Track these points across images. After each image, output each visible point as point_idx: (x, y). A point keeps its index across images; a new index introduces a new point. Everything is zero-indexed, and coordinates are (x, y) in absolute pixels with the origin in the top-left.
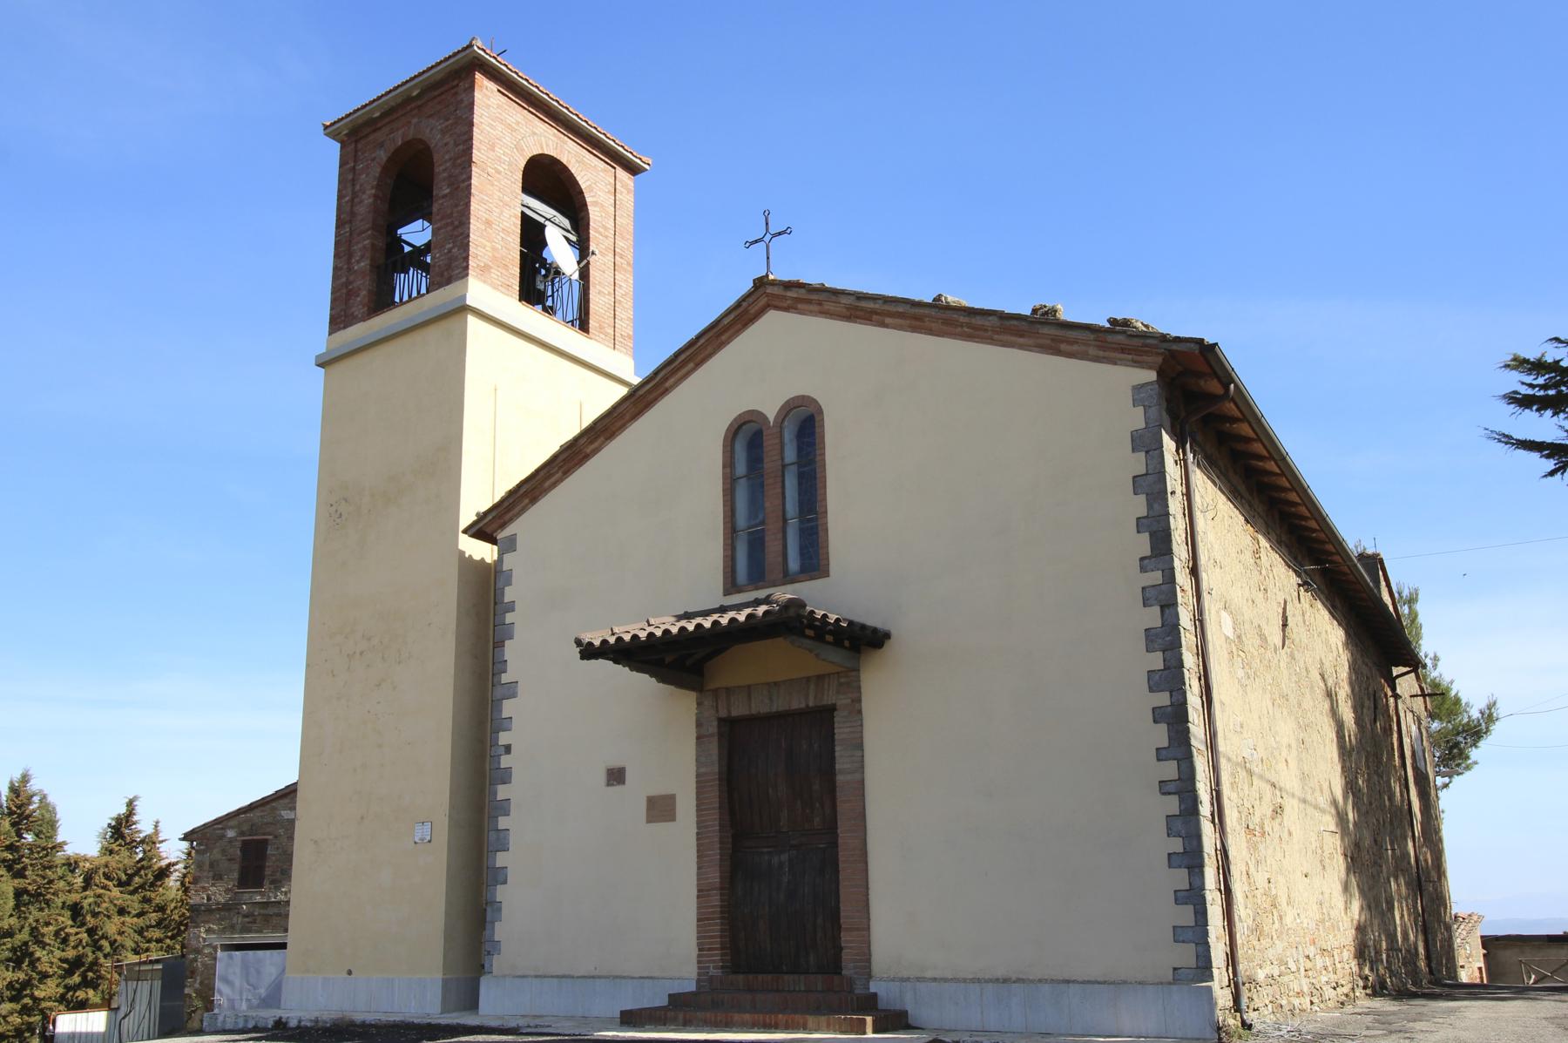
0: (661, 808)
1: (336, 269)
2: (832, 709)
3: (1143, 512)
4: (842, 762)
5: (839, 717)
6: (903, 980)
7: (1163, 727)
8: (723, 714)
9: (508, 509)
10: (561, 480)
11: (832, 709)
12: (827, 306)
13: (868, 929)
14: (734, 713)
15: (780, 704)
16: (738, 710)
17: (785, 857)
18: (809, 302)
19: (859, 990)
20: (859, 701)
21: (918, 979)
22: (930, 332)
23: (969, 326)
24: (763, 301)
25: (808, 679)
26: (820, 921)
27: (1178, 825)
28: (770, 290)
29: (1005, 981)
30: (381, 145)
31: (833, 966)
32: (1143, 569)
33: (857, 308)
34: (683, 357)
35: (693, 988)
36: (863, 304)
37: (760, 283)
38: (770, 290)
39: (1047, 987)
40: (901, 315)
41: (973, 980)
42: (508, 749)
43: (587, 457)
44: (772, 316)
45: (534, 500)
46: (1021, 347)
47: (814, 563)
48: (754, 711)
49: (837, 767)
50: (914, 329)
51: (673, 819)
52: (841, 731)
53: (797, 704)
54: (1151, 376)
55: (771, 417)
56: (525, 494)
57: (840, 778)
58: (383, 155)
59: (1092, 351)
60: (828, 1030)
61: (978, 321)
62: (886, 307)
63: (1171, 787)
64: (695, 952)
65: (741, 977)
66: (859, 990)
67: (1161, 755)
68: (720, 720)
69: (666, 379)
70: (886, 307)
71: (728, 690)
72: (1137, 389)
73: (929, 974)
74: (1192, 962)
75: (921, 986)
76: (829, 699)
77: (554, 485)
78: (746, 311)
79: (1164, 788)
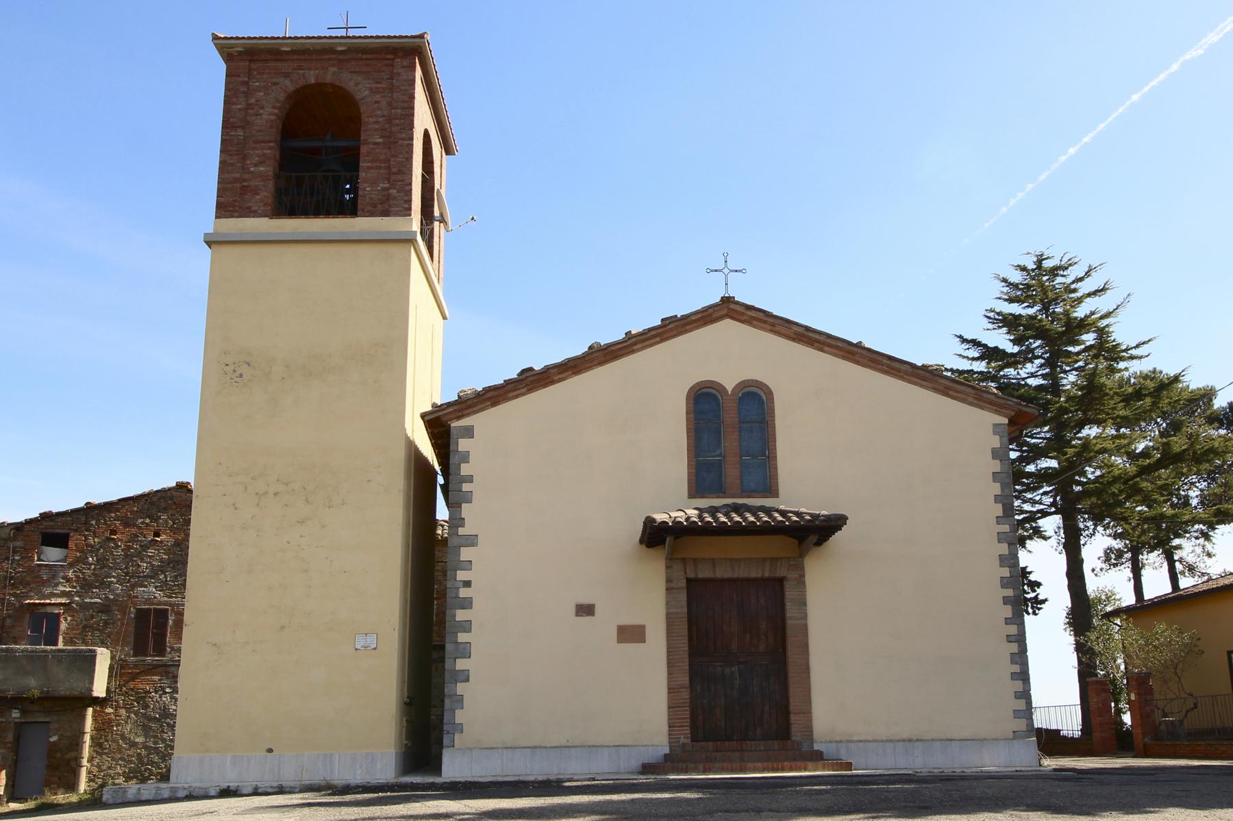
0: (631, 634)
1: (223, 163)
2: (781, 581)
3: (999, 492)
4: (791, 610)
5: (788, 586)
6: (837, 742)
7: (1009, 607)
8: (691, 575)
9: (470, 407)
10: (524, 394)
11: (781, 581)
12: (778, 328)
13: (810, 712)
14: (701, 575)
15: (741, 572)
16: (705, 573)
17: (735, 669)
18: (765, 322)
19: (805, 748)
20: (803, 576)
21: (849, 741)
22: (857, 363)
23: (888, 366)
24: (725, 312)
25: (764, 560)
26: (767, 708)
27: (1017, 658)
28: (732, 306)
29: (910, 740)
30: (287, 75)
31: (784, 733)
32: (998, 523)
33: (803, 335)
34: (654, 333)
35: (1077, 734)
36: (811, 334)
37: (727, 300)
38: (732, 306)
39: (938, 744)
40: (837, 347)
41: (887, 741)
42: (467, 584)
43: (553, 382)
44: (728, 322)
45: (494, 404)
46: (921, 386)
47: (770, 489)
48: (736, 576)
49: (788, 615)
50: (844, 358)
51: (644, 641)
52: (790, 593)
53: (755, 573)
54: (1006, 421)
55: (730, 389)
56: (490, 399)
57: (789, 622)
58: (289, 85)
59: (970, 399)
60: (824, 769)
61: (897, 365)
62: (829, 341)
63: (1013, 639)
64: (665, 729)
65: (710, 743)
66: (805, 748)
67: (1008, 621)
68: (689, 580)
69: (635, 344)
70: (829, 341)
71: (695, 560)
72: (996, 425)
73: (855, 738)
74: (1024, 728)
75: (852, 745)
76: (781, 572)
77: (517, 397)
78: (710, 315)
79: (1009, 639)
